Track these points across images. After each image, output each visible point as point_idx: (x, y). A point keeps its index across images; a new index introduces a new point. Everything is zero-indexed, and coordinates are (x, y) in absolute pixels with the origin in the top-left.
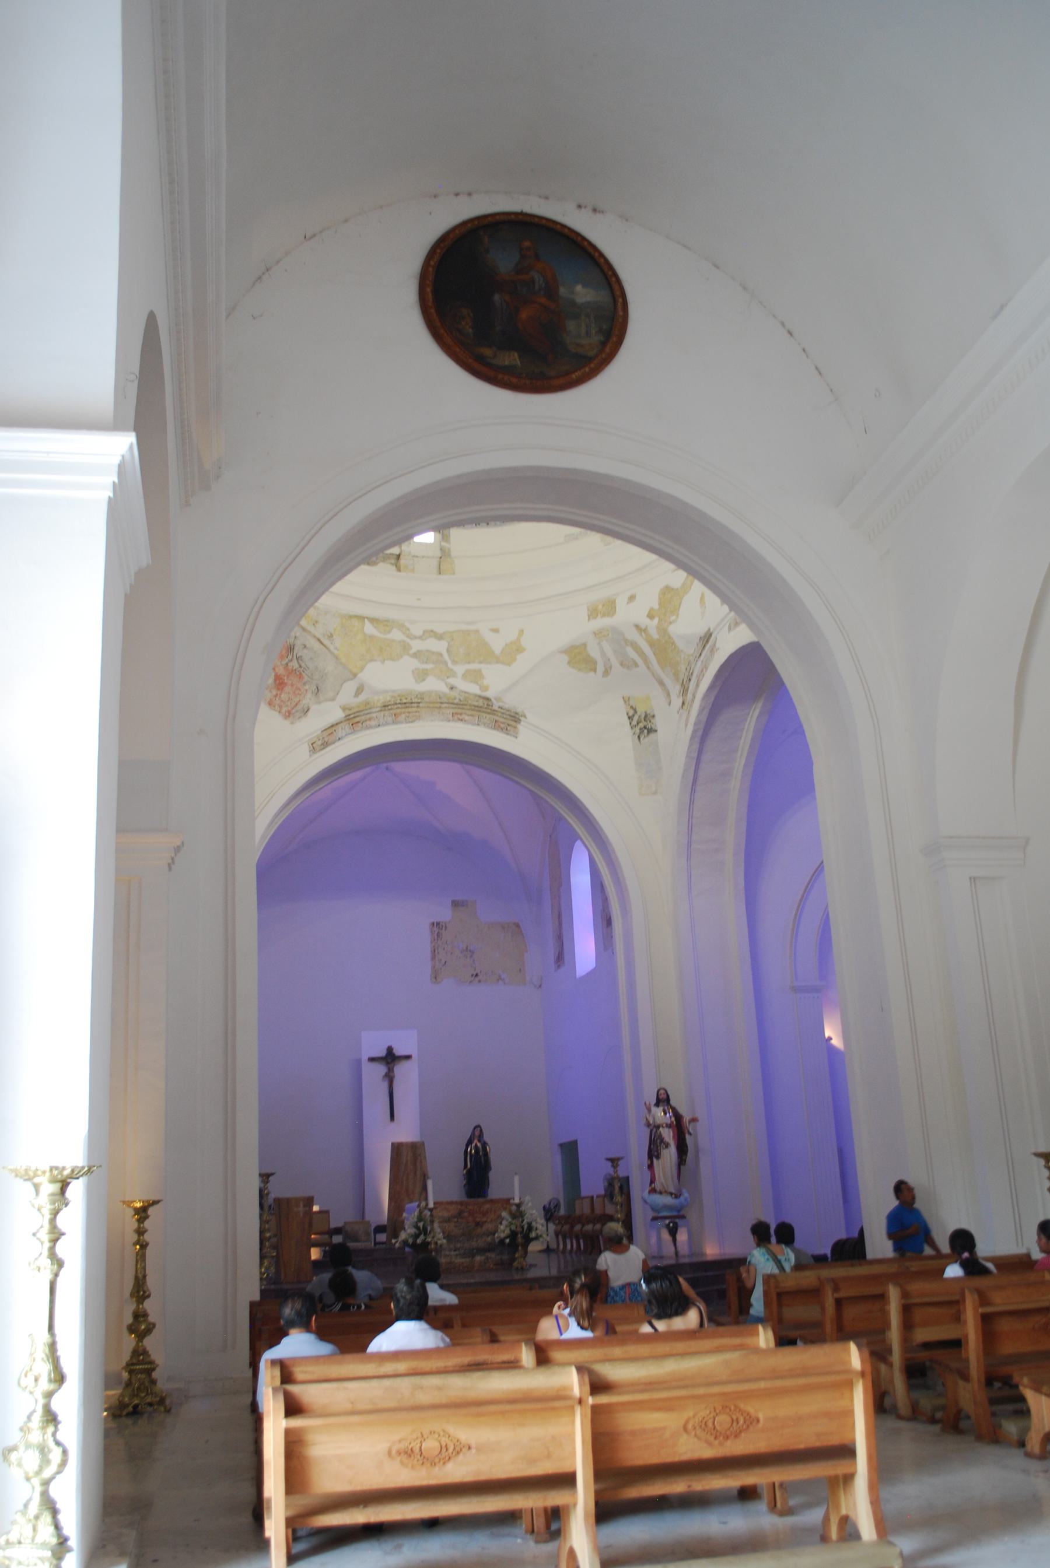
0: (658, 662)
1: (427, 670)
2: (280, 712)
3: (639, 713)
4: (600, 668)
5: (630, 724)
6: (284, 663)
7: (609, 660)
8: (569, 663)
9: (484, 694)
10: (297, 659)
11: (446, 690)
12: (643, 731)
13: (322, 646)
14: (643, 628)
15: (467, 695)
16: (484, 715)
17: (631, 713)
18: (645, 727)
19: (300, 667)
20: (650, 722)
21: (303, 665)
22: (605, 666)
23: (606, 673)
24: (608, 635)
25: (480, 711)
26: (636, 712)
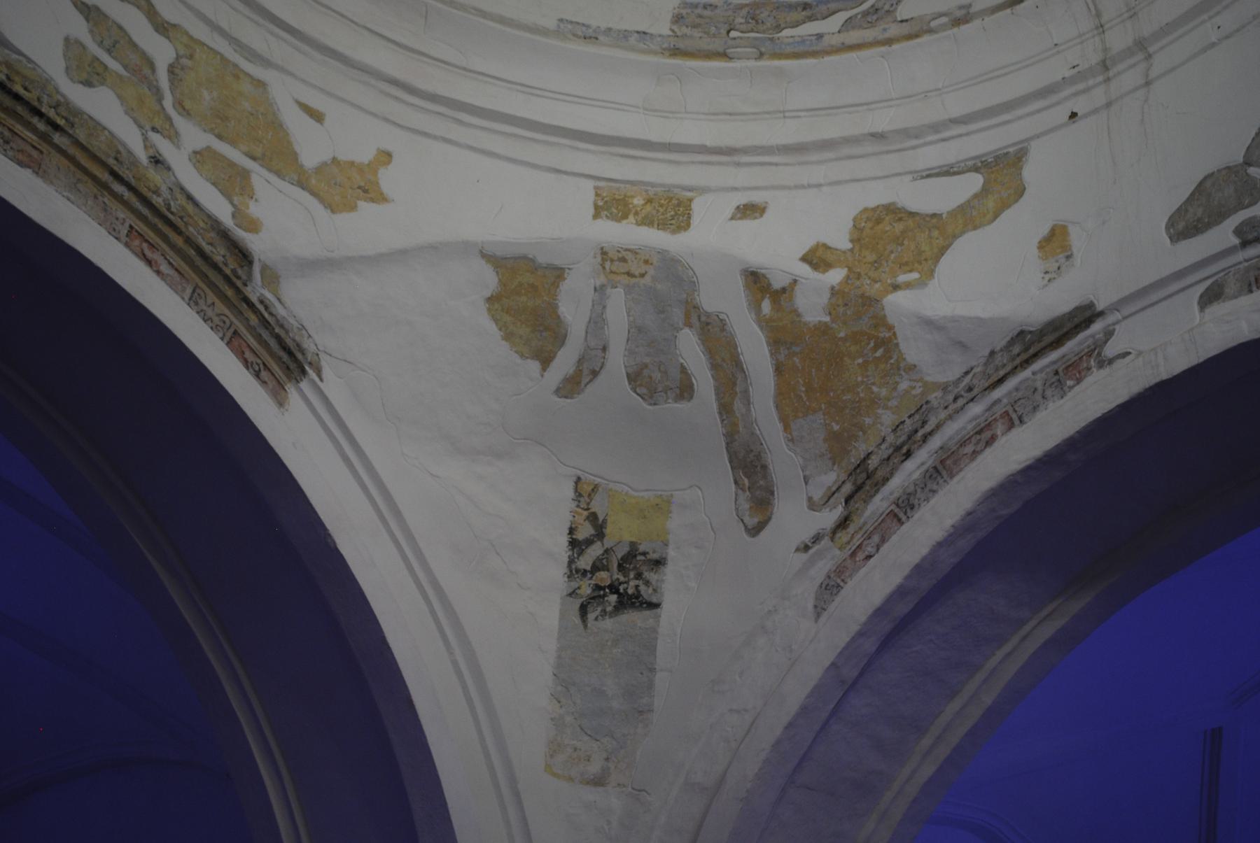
0: (782, 395)
1: (106, 67)
3: (608, 542)
4: (565, 361)
5: (571, 562)
7: (604, 349)
8: (490, 300)
9: (240, 234)
11: (142, 156)
12: (605, 595)
14: (777, 284)
15: (190, 208)
16: (211, 297)
17: (585, 531)
18: (614, 588)
20: (639, 576)
22: (580, 361)
23: (571, 386)
24: (642, 275)
25: (204, 277)
26: (600, 534)
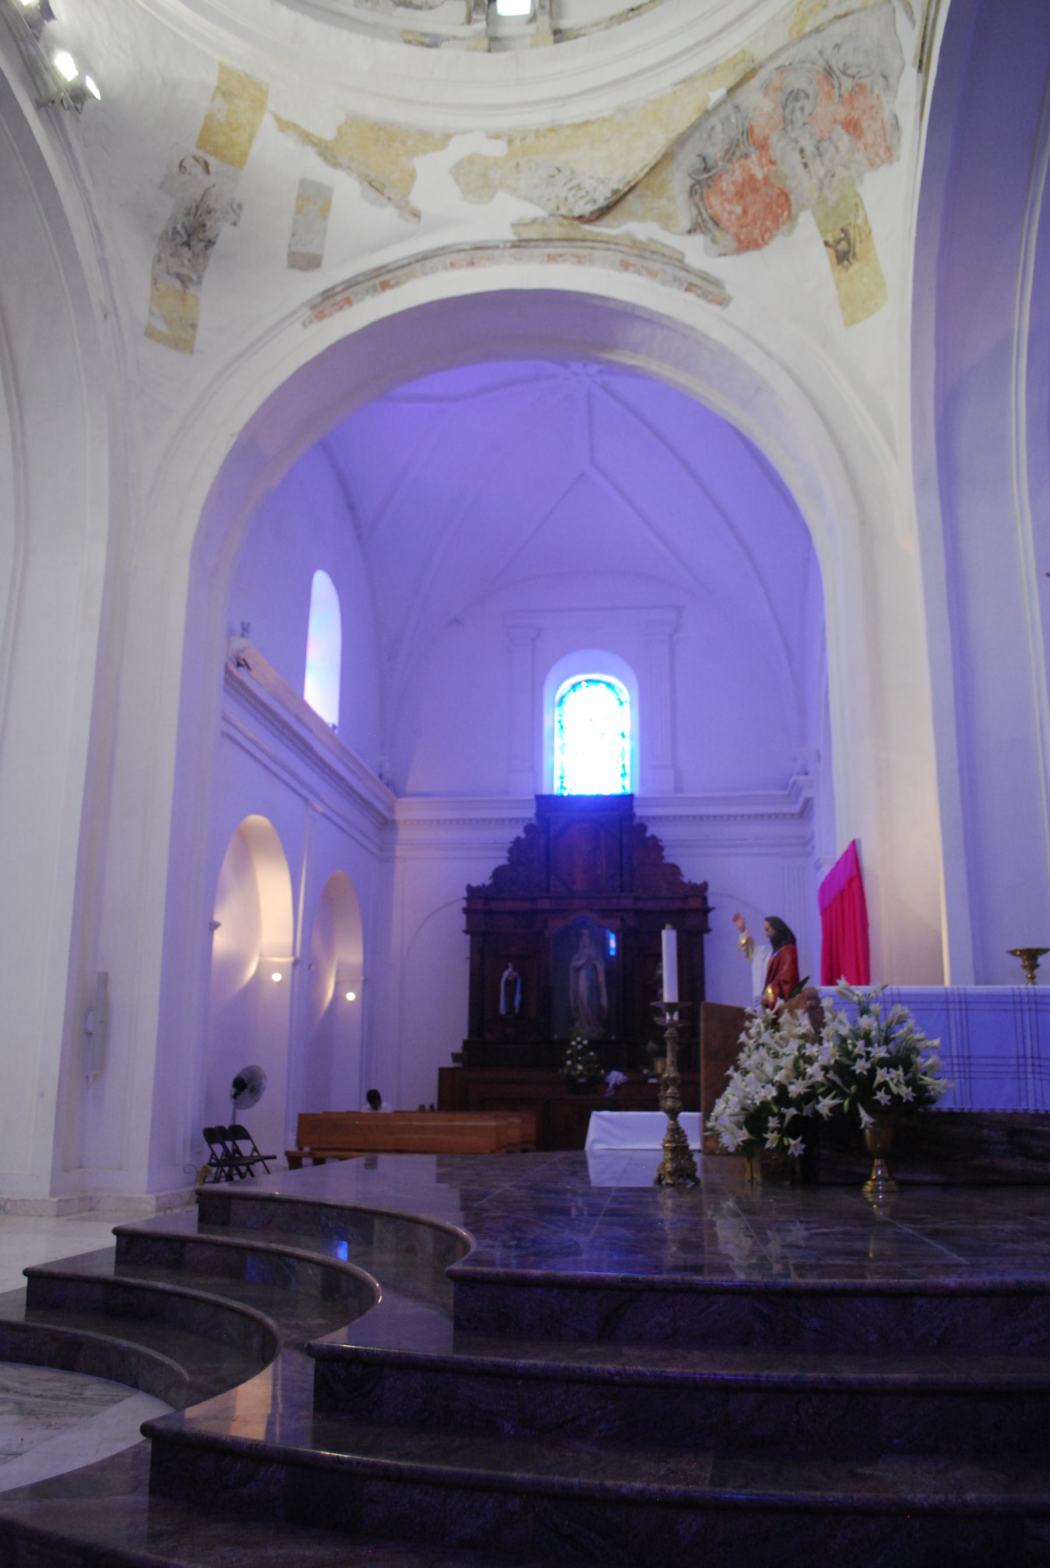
2: (883, 162)
6: (836, 99)
10: (843, 73)
13: (850, 18)
19: (854, 77)
21: (853, 71)
